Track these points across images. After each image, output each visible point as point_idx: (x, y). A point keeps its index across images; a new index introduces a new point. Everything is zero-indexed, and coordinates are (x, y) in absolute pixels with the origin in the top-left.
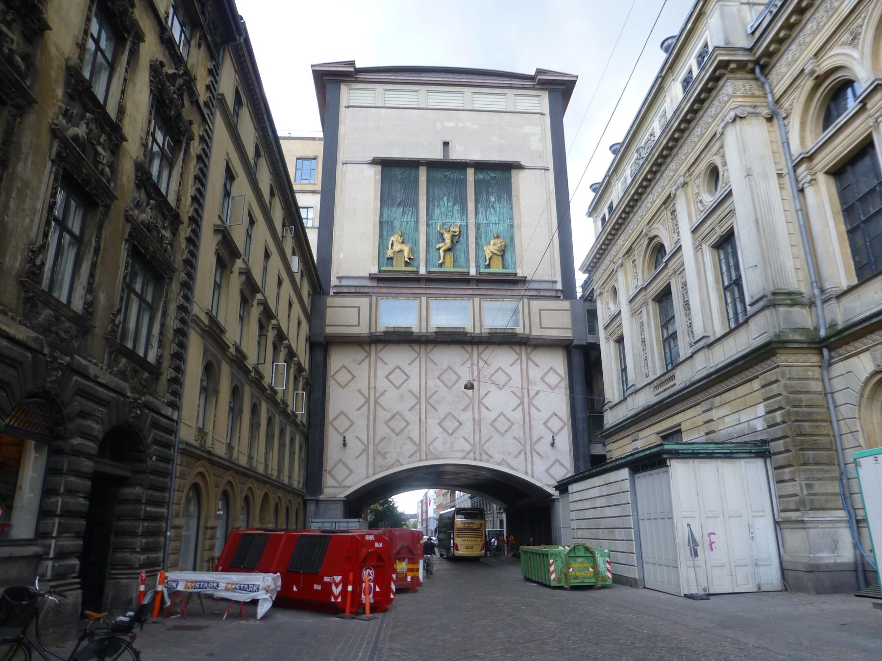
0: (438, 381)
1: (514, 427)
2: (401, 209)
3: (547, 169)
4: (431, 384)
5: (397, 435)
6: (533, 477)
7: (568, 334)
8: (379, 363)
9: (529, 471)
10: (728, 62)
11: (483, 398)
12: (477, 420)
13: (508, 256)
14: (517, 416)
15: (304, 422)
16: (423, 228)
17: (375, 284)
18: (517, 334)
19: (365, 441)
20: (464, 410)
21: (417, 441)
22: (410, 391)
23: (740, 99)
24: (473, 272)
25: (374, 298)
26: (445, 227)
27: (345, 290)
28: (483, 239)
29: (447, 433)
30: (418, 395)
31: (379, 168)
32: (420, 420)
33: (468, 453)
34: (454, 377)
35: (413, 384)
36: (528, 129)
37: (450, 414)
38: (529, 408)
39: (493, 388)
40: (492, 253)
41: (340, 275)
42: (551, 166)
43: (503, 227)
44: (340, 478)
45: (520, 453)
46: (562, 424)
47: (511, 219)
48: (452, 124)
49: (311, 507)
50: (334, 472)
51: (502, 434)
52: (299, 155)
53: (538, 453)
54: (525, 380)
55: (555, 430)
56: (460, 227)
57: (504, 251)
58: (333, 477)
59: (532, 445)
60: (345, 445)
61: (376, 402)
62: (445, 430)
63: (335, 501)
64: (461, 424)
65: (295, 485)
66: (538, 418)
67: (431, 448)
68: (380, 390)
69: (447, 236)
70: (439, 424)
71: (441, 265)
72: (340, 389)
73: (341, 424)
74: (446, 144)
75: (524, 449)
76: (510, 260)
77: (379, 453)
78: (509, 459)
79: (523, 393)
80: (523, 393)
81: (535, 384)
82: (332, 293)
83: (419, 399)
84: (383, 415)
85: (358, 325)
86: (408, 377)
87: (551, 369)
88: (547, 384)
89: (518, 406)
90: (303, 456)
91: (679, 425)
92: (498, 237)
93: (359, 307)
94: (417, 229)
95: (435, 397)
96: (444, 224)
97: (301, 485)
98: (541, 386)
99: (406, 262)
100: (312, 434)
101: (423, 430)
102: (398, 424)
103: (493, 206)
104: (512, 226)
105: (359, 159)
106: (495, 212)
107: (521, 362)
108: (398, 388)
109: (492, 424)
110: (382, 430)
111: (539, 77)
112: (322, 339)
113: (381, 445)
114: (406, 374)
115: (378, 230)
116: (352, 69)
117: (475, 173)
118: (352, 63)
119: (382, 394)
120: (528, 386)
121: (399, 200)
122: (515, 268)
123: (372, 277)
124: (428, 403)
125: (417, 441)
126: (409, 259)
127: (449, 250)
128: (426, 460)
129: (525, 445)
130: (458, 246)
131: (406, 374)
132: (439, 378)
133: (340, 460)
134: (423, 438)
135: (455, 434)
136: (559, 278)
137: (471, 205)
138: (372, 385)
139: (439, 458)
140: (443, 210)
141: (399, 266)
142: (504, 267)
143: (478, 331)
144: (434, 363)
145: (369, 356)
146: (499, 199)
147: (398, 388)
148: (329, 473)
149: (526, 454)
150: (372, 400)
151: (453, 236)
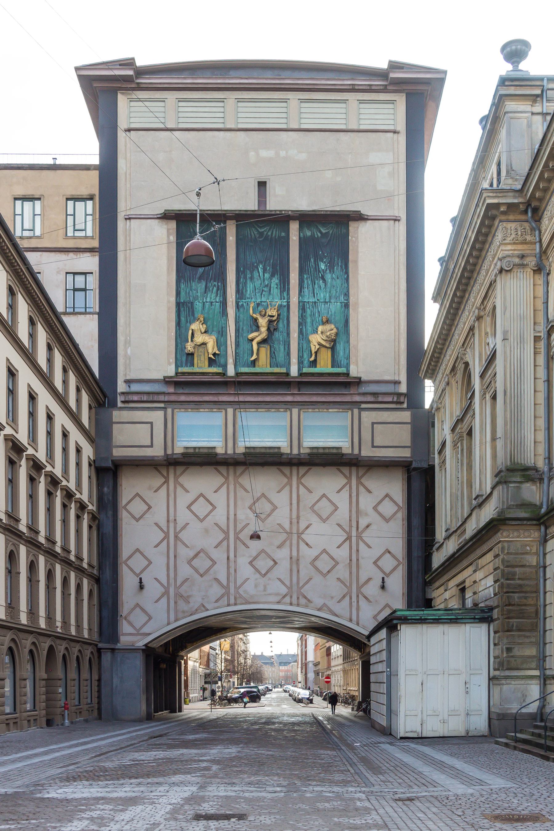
1: (340, 567)
3: (396, 220)
5: (201, 576)
7: (406, 454)
9: (354, 618)
12: (294, 559)
13: (340, 347)
14: (343, 554)
19: (165, 582)
21: (225, 583)
26: (260, 308)
29: (260, 573)
31: (173, 225)
34: (268, 507)
36: (374, 158)
39: (314, 519)
40: (320, 344)
41: (128, 378)
43: (335, 307)
45: (344, 597)
47: (347, 294)
48: (270, 153)
49: (107, 658)
50: (131, 618)
51: (325, 575)
53: (365, 597)
55: (387, 570)
56: (280, 306)
57: (334, 341)
59: (359, 588)
60: (141, 587)
61: (176, 537)
62: (257, 570)
64: (276, 563)
66: (367, 555)
67: (241, 591)
68: (180, 523)
69: (263, 322)
70: (251, 563)
71: (254, 363)
72: (134, 522)
73: (137, 563)
74: (262, 185)
75: (349, 593)
76: (341, 353)
77: (182, 596)
78: (330, 604)
79: (351, 526)
80: (351, 526)
81: (366, 514)
82: (120, 404)
84: (184, 553)
85: (152, 446)
92: (328, 322)
93: (151, 423)
94: (224, 313)
96: (258, 305)
101: (232, 571)
102: (202, 563)
103: (323, 278)
104: (347, 306)
109: (313, 563)
110: (185, 571)
111: (392, 75)
113: (184, 587)
114: (211, 504)
117: (301, 229)
120: (357, 517)
122: (348, 366)
123: (167, 381)
125: (225, 583)
126: (214, 354)
130: (277, 335)
131: (211, 504)
134: (232, 579)
135: (269, 575)
136: (403, 378)
138: (172, 518)
140: (258, 283)
141: (201, 366)
142: (334, 364)
146: (331, 267)
149: (351, 598)
151: (270, 322)
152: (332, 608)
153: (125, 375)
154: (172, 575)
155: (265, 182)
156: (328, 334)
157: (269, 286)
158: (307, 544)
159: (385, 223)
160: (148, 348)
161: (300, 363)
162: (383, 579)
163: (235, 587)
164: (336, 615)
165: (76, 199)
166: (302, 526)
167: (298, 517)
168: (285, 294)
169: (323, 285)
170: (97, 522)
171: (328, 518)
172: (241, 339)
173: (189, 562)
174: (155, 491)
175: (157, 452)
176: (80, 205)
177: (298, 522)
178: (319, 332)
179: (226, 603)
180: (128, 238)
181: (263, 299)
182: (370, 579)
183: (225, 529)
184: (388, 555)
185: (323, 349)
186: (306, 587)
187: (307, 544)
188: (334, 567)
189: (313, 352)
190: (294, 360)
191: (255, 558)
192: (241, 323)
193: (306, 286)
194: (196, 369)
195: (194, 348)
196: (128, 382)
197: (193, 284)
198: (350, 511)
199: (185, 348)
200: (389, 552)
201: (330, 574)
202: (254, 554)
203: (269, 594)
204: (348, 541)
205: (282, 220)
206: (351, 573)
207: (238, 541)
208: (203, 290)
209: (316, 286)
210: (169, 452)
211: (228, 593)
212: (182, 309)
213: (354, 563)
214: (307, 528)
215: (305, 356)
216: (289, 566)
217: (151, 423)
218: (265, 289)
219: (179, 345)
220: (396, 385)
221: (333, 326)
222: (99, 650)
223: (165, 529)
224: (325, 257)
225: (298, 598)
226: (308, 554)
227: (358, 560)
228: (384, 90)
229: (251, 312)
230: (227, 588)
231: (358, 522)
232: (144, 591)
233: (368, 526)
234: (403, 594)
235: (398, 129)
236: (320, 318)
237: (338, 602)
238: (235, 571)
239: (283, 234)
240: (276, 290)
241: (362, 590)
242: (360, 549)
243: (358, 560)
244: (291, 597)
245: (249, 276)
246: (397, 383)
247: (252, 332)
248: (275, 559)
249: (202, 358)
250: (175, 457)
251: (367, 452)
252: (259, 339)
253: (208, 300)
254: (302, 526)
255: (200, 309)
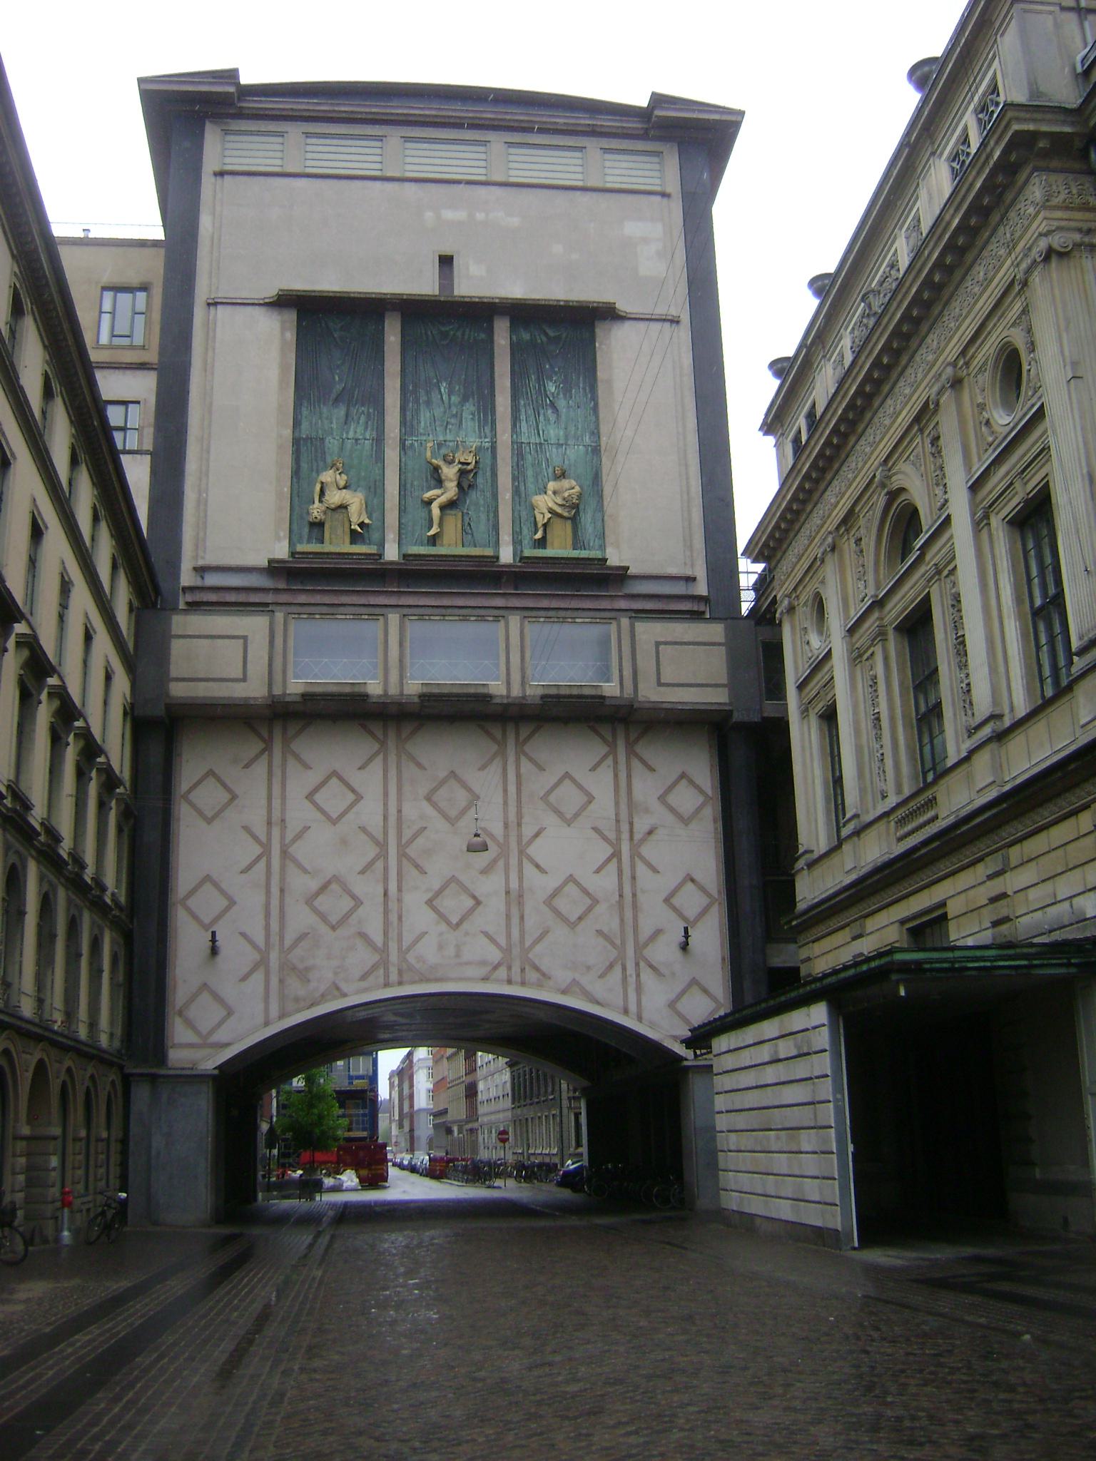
0: (425, 804)
1: (599, 909)
2: (341, 411)
3: (675, 321)
4: (410, 811)
5: (333, 928)
6: (640, 1019)
7: (719, 697)
8: (291, 762)
9: (633, 1007)
10: (1035, 135)
11: (530, 842)
12: (514, 895)
13: (587, 519)
14: (605, 884)
15: (123, 899)
16: (392, 455)
17: (282, 585)
18: (603, 697)
19: (260, 940)
20: (485, 871)
21: (378, 939)
22: (363, 829)
23: (1059, 214)
24: (506, 556)
25: (279, 616)
26: (443, 451)
27: (213, 597)
28: (530, 479)
29: (448, 923)
30: (380, 837)
31: (291, 316)
32: (386, 894)
33: (496, 968)
34: (461, 797)
35: (370, 813)
36: (633, 229)
37: (453, 879)
38: (633, 867)
39: (550, 820)
40: (551, 511)
41: (201, 563)
42: (685, 318)
43: (575, 453)
44: (204, 1027)
45: (611, 966)
46: (705, 901)
47: (596, 433)
48: (461, 215)
49: (141, 1094)
50: (192, 1013)
51: (572, 925)
52: (106, 279)
53: (651, 966)
54: (623, 807)
55: (691, 913)
56: (479, 449)
57: (576, 507)
58: (190, 1024)
59: (639, 948)
60: (214, 951)
61: (285, 853)
62: (442, 916)
63: (192, 1078)
64: (478, 903)
65: (104, 1040)
66: (652, 886)
67: (411, 958)
68: (293, 828)
69: (450, 472)
70: (430, 903)
71: (433, 540)
72: (203, 824)
73: (207, 903)
74: (446, 261)
75: (621, 958)
76: (590, 529)
77: (294, 968)
78: (587, 981)
79: (618, 831)
80: (618, 831)
81: (647, 811)
82: (182, 606)
83: (382, 846)
84: (301, 884)
85: (244, 679)
86: (359, 797)
87: (683, 776)
88: (672, 809)
89: (608, 860)
90: (121, 978)
91: (943, 904)
92: (563, 475)
93: (245, 638)
94: (380, 458)
95: (420, 841)
96: (440, 445)
97: (117, 1044)
98: (659, 815)
99: (353, 532)
100: (139, 925)
101: (393, 917)
102: (335, 904)
103: (553, 405)
104: (596, 450)
105: (245, 294)
106: (558, 416)
107: (616, 762)
108: (334, 822)
109: (549, 901)
110: (300, 918)
111: (658, 113)
112: (160, 711)
113: (298, 951)
114: (353, 791)
115: (288, 459)
116: (232, 89)
117: (513, 328)
118: (232, 75)
119: (299, 836)
120: (631, 816)
121: (339, 387)
122: (603, 547)
123: (275, 569)
124: (402, 855)
125: (378, 939)
126: (362, 525)
127: (448, 507)
128: (400, 983)
129: (622, 949)
130: (473, 496)
131: (353, 791)
132: (428, 798)
133: (205, 986)
134: (393, 934)
135: (465, 926)
136: (700, 572)
137: (503, 401)
138: (276, 815)
139: (428, 980)
140: (438, 412)
141: (337, 543)
142: (577, 543)
143: (516, 692)
144: (419, 765)
145: (268, 749)
146: (567, 392)
147: (334, 822)
148: (180, 1013)
149: (624, 969)
150: (277, 850)
151: (462, 473)
152: (589, 988)
153: (196, 557)
154: (275, 926)
155: (451, 258)
156: (566, 494)
157: (459, 416)
158: (538, 866)
159: (656, 326)
160: (236, 511)
161: (517, 542)
162: (686, 929)
163: (400, 949)
164: (598, 1003)
165: (117, 289)
166: (528, 831)
167: (520, 815)
168: (488, 429)
169: (552, 418)
170: (132, 821)
171: (577, 815)
172: (409, 500)
173: (310, 901)
174: (247, 766)
175: (254, 690)
176: (124, 298)
177: (519, 825)
178: (550, 492)
179: (381, 980)
180: (211, 334)
181: (449, 437)
182: (658, 932)
183: (380, 837)
184: (690, 886)
185: (557, 521)
186: (538, 948)
187: (538, 866)
188: (590, 909)
189: (540, 525)
190: (506, 537)
191: (438, 893)
192: (410, 475)
193: (523, 417)
194: (327, 548)
195: (325, 513)
196: (201, 570)
197: (325, 410)
198: (617, 804)
199: (308, 513)
200: (693, 880)
201: (583, 923)
202: (436, 886)
203: (467, 963)
204: (615, 860)
205: (480, 314)
206: (622, 920)
207: (405, 861)
208: (342, 420)
209: (542, 418)
210: (277, 691)
211: (384, 963)
212: (303, 449)
213: (628, 902)
214: (537, 835)
215: (525, 531)
216: (503, 908)
217: (245, 638)
218: (453, 421)
219: (297, 508)
220: (690, 584)
221: (574, 483)
222: (127, 1080)
223: (263, 838)
224: (556, 373)
225: (523, 970)
226: (540, 885)
227: (634, 895)
228: (644, 136)
229: (429, 454)
230: (385, 950)
231: (631, 824)
232: (219, 958)
233: (650, 833)
234: (723, 959)
235: (668, 190)
236: (550, 470)
237: (601, 976)
238: (400, 918)
239: (483, 336)
240: (470, 424)
241: (646, 952)
242: (638, 874)
243: (634, 895)
244: (509, 968)
245: (423, 398)
246: (691, 580)
247: (429, 489)
248: (477, 894)
249: (340, 532)
250: (288, 699)
251: (650, 693)
252: (443, 499)
253: (351, 435)
254: (528, 831)
255: (336, 450)
